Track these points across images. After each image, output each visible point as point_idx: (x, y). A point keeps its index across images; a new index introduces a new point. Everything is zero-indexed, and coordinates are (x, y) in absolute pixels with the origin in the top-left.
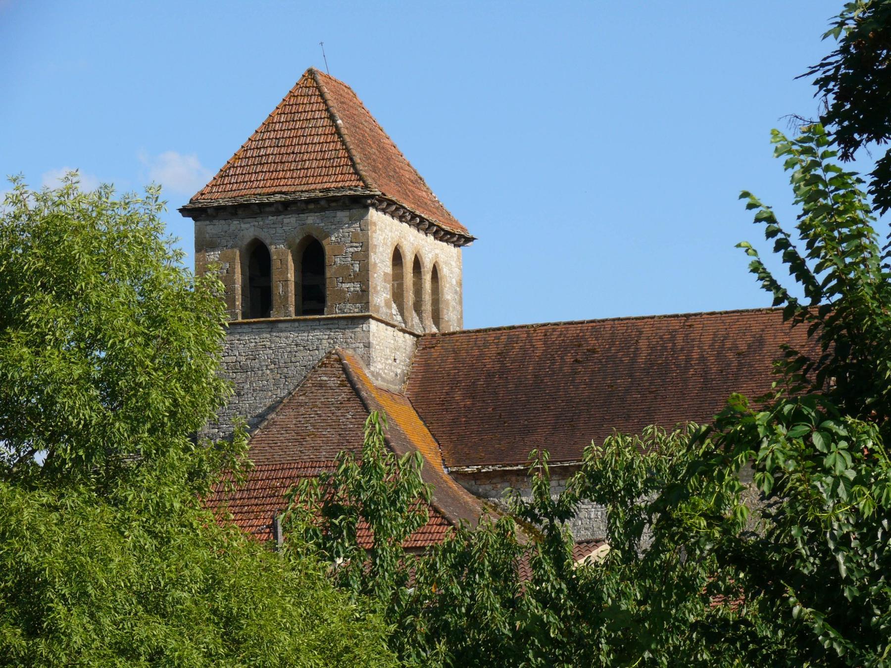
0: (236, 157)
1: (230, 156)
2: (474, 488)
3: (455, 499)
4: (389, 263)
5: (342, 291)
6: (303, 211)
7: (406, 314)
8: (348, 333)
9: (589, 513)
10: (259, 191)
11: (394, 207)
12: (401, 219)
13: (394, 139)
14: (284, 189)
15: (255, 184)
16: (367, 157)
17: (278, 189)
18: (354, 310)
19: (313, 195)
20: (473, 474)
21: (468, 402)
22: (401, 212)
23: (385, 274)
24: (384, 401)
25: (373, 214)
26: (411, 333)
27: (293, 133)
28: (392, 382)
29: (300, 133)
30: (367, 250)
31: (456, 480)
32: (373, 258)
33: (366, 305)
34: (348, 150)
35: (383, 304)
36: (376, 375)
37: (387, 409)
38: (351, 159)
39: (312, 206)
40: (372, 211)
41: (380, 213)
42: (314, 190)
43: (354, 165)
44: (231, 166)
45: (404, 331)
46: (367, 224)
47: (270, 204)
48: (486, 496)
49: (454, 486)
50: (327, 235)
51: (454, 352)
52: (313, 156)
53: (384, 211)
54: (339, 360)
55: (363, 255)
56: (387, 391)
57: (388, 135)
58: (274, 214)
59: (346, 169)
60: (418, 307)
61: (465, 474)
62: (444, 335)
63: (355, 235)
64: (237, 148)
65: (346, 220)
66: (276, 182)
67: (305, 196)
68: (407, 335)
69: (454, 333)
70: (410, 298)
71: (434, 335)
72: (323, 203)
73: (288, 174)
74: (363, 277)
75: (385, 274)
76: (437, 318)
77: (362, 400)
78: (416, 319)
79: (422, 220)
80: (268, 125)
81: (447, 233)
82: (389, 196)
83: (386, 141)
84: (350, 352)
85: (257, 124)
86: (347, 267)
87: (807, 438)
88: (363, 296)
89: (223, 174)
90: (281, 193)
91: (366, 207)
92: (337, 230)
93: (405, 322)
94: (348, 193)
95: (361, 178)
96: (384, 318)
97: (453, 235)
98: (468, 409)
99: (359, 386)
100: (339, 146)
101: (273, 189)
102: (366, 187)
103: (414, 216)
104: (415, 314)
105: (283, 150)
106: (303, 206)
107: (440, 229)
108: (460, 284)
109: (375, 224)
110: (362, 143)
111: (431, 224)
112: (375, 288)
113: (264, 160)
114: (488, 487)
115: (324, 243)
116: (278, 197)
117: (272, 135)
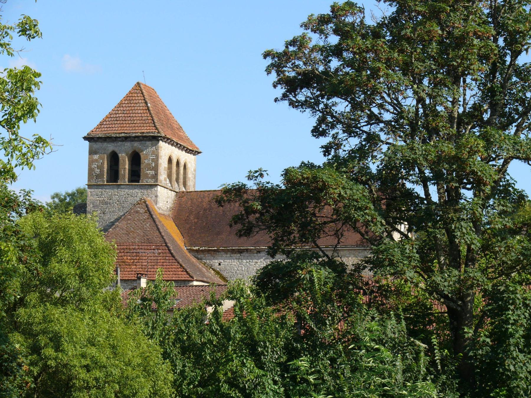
0: (107, 117)
1: (104, 116)
2: (197, 256)
3: (189, 260)
4: (166, 163)
5: (147, 174)
6: (133, 141)
7: (172, 183)
8: (149, 191)
9: (242, 268)
10: (115, 132)
11: (169, 141)
12: (172, 145)
13: (171, 111)
14: (126, 131)
15: (114, 129)
16: (160, 119)
17: (123, 131)
18: (151, 182)
19: (137, 135)
20: (196, 250)
21: (196, 220)
22: (172, 142)
23: (165, 167)
24: (162, 219)
25: (161, 143)
26: (174, 191)
27: (130, 108)
28: (166, 211)
29: (133, 108)
30: (158, 158)
31: (189, 252)
32: (160, 161)
33: (157, 180)
34: (152, 117)
35: (163, 179)
36: (159, 208)
37: (163, 222)
38: (153, 121)
39: (136, 139)
40: (161, 142)
41: (164, 143)
42: (138, 133)
43: (154, 123)
44: (104, 120)
45: (171, 190)
46: (158, 147)
47: (120, 137)
48: (201, 259)
49: (188, 254)
50: (142, 151)
51: (191, 199)
52: (138, 118)
53: (165, 142)
54: (145, 202)
55: (156, 160)
56: (164, 215)
57: (169, 109)
58: (121, 141)
59: (151, 125)
60: (177, 180)
61: (193, 250)
62: (187, 192)
63: (153, 151)
64: (107, 113)
65: (150, 145)
66: (123, 128)
67: (134, 135)
68: (172, 192)
69: (191, 192)
70: (174, 176)
71: (183, 192)
72: (141, 138)
73: (128, 125)
74: (156, 169)
75: (165, 167)
76: (185, 184)
77: (153, 219)
78: (176, 185)
79: (181, 145)
80: (120, 105)
81: (190, 150)
82: (168, 136)
83: (167, 111)
84: (149, 199)
85: (116, 104)
86: (150, 164)
87: (243, 360)
88: (155, 177)
89: (101, 124)
90: (124, 133)
91: (158, 141)
92: (146, 149)
93: (172, 187)
94: (151, 135)
95: (157, 129)
96: (163, 185)
97: (193, 151)
98: (196, 223)
99: (152, 213)
100: (148, 115)
101: (121, 131)
102: (159, 132)
103: (177, 144)
104: (176, 183)
105: (126, 115)
106: (133, 139)
107: (188, 149)
108: (195, 171)
109: (161, 147)
110: (158, 113)
111: (184, 147)
112: (160, 173)
113: (118, 119)
114: (202, 256)
115: (141, 154)
116: (123, 135)
117: (122, 109)
